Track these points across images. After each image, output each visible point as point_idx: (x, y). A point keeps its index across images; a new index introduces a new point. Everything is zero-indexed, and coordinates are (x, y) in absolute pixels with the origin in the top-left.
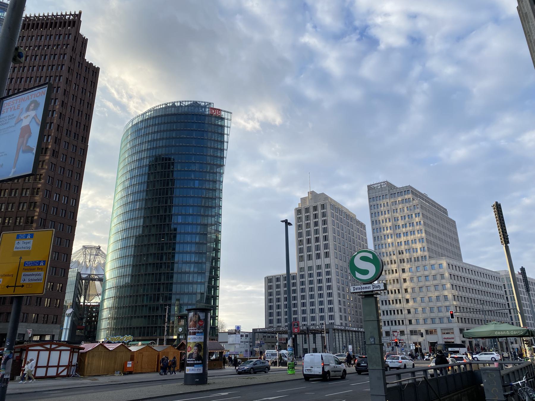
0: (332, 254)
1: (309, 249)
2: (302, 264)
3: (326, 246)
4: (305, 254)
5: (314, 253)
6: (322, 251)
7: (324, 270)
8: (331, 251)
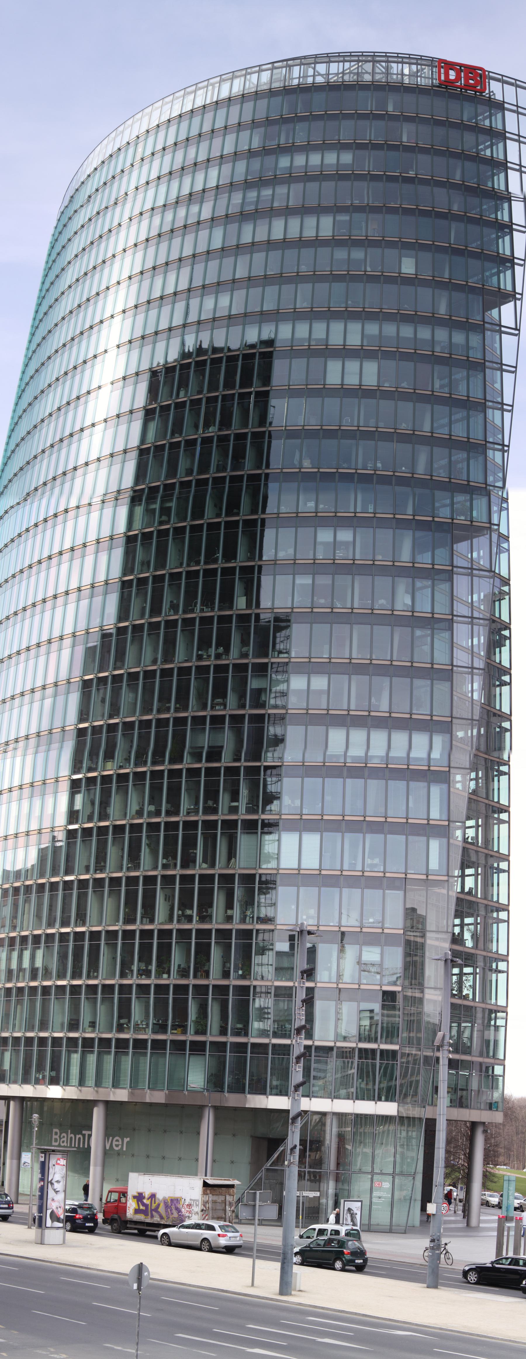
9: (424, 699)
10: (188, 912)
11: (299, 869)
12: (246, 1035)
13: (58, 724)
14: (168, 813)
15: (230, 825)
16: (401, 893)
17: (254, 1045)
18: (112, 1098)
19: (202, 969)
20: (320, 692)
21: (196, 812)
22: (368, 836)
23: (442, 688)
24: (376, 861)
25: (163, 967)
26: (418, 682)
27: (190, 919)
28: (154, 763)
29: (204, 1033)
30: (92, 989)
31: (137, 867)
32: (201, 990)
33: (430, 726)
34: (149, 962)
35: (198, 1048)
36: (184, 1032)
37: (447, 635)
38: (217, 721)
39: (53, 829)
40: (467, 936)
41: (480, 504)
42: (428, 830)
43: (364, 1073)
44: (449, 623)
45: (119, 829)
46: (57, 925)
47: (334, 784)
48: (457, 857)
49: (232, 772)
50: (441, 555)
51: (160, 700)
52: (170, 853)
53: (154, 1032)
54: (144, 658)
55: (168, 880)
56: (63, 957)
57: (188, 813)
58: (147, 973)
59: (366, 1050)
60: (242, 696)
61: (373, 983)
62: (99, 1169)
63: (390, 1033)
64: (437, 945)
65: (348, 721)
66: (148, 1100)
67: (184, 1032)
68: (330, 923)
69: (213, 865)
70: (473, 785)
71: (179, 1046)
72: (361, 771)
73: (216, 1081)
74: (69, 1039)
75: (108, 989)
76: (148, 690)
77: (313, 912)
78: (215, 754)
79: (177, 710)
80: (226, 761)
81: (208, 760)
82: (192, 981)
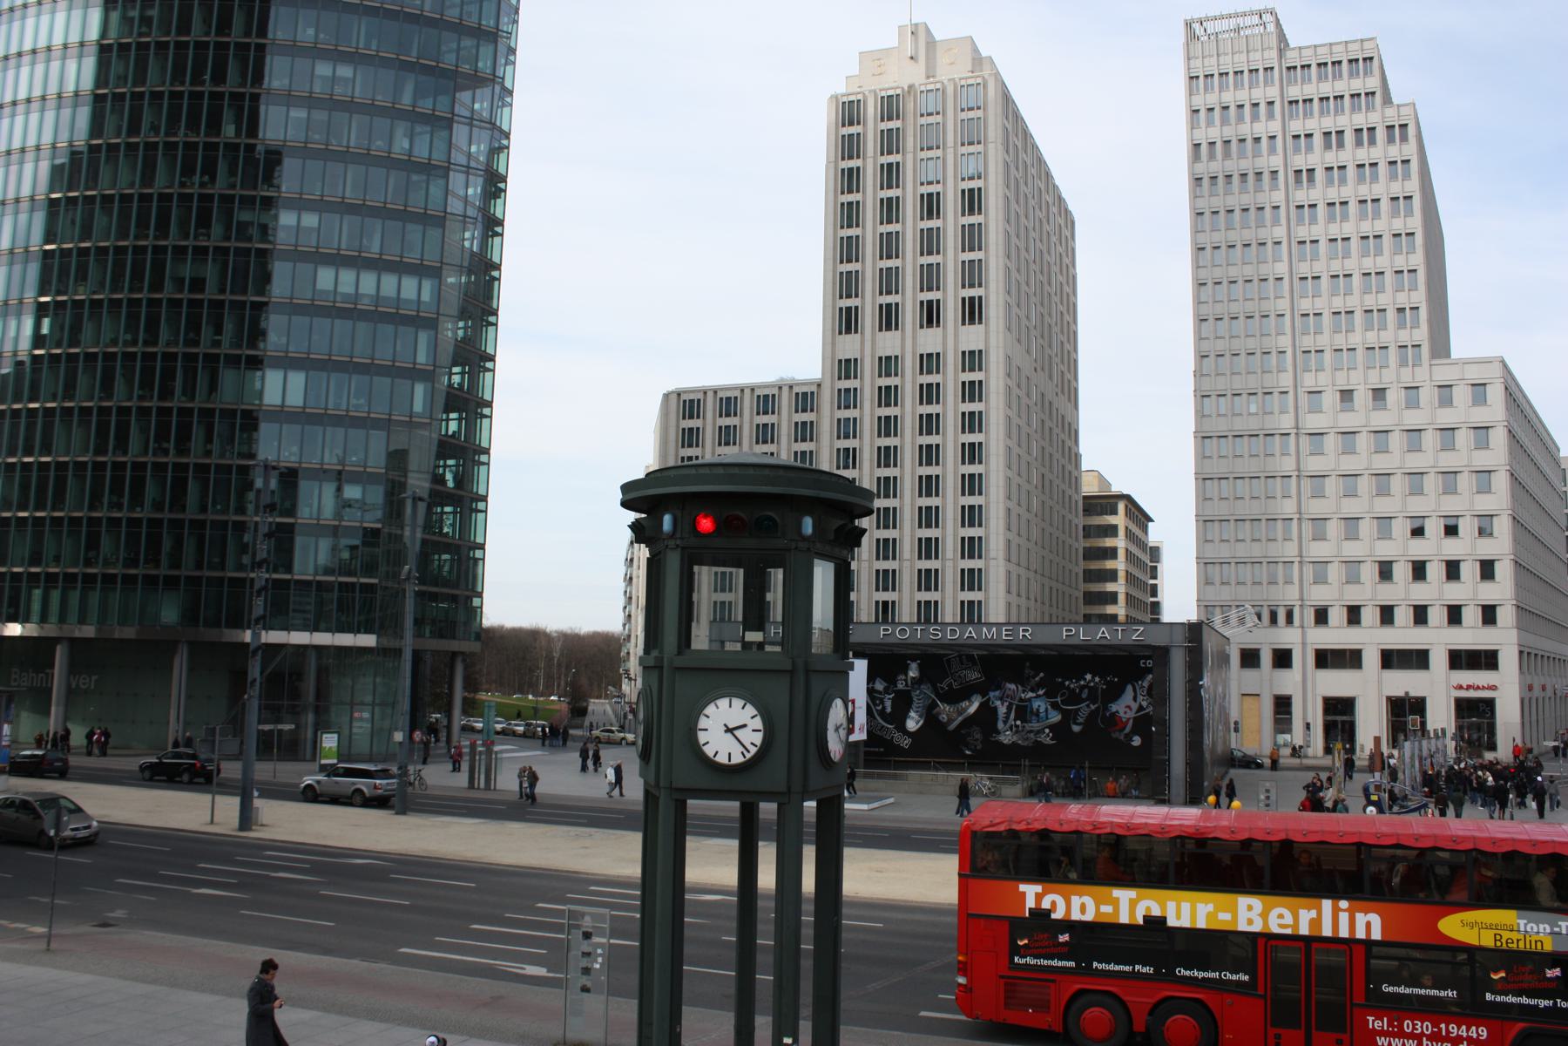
0: (994, 310)
1: (889, 280)
2: (849, 346)
3: (972, 274)
4: (869, 303)
5: (910, 299)
6: (951, 297)
7: (951, 378)
8: (994, 295)
9: (417, 243)
10: (165, 445)
11: (283, 406)
12: (223, 569)
13: (20, 243)
14: (146, 343)
15: (212, 359)
16: (384, 434)
17: (231, 579)
18: (77, 634)
19: (178, 502)
20: (311, 229)
21: (176, 344)
22: (355, 378)
23: (434, 233)
24: (362, 401)
25: (137, 499)
26: (410, 227)
27: (166, 452)
28: (131, 290)
29: (178, 567)
30: (57, 522)
31: (109, 397)
32: (176, 524)
33: (420, 270)
34: (121, 495)
35: (171, 583)
36: (157, 566)
37: (442, 182)
38: (201, 252)
39: (15, 353)
40: (449, 477)
41: (486, 51)
42: (415, 374)
43: (343, 607)
44: (445, 170)
45: (90, 358)
46: (20, 453)
47: (322, 324)
48: (440, 402)
49: (217, 305)
50: (443, 101)
51: (137, 226)
52: (146, 384)
53: (126, 566)
54: (120, 181)
55: (144, 412)
56: (25, 487)
57: (168, 345)
58: (119, 507)
59: (347, 584)
60: (228, 228)
61: (352, 519)
62: (61, 709)
63: (369, 569)
64: (418, 483)
65: (338, 260)
66: (116, 636)
67: (157, 566)
68: (311, 462)
69: (192, 399)
70: (461, 333)
71: (151, 581)
72: (348, 311)
73: (191, 616)
74: (30, 574)
75: (74, 522)
76: (124, 216)
77: (295, 449)
78: (198, 284)
79: (156, 238)
80: (210, 293)
81: (191, 291)
82: (166, 515)
